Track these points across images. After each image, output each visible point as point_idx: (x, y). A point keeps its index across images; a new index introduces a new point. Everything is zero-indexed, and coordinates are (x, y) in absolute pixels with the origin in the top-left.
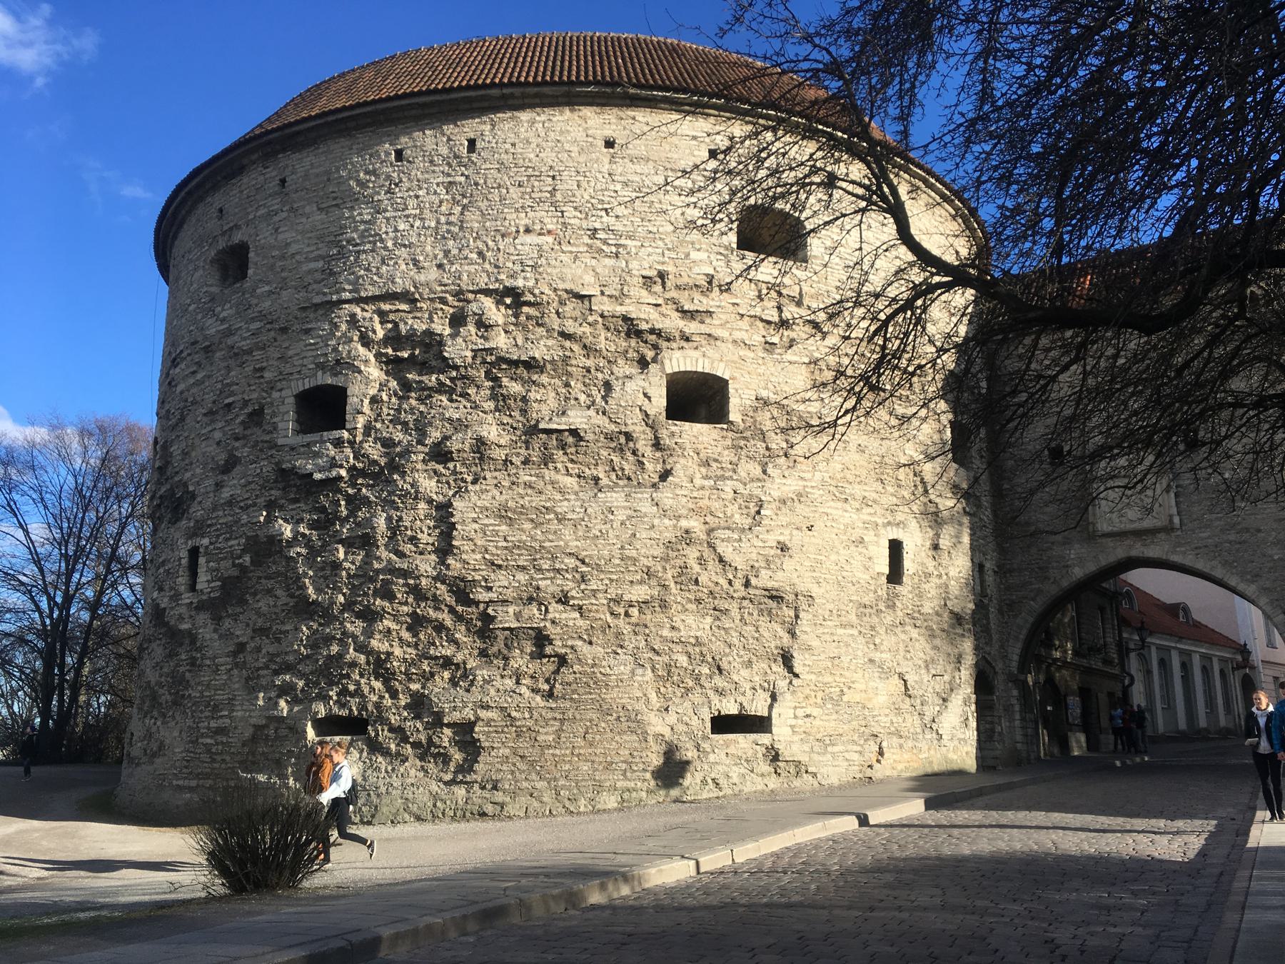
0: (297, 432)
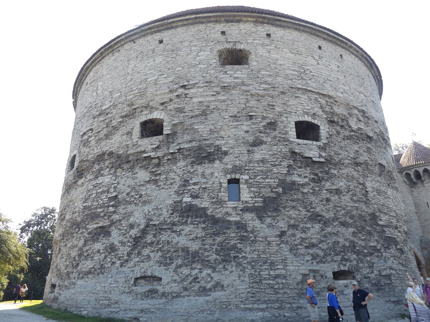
0: (298, 137)
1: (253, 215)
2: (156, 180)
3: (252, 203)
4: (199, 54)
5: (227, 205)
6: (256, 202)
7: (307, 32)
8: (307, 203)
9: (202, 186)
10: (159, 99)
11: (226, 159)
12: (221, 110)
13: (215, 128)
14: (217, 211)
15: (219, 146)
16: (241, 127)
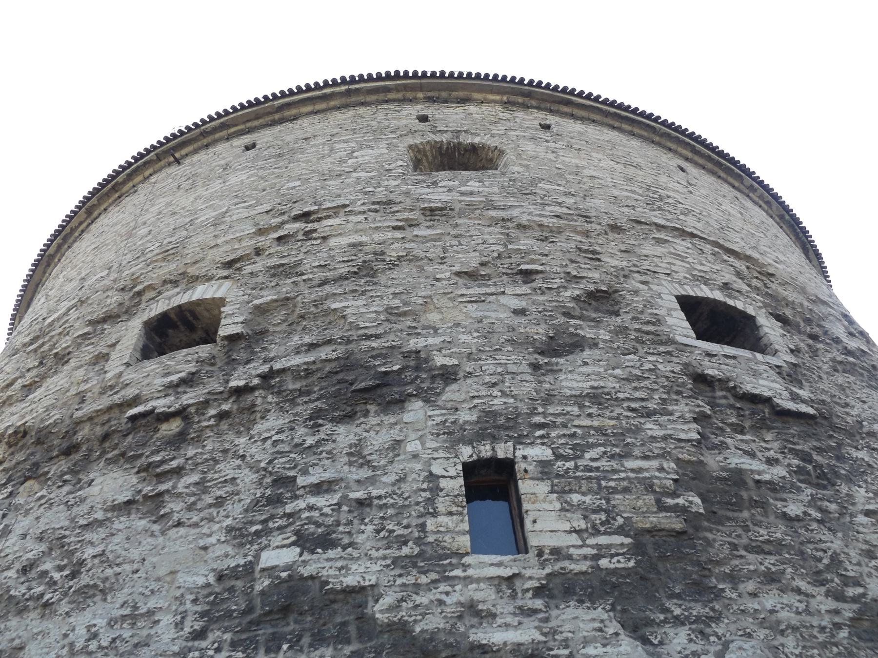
1: (599, 613)
2: (160, 494)
3: (585, 557)
4: (355, 154)
5: (470, 572)
6: (602, 552)
7: (640, 137)
8: (820, 560)
9: (353, 495)
10: (221, 255)
11: (452, 393)
12: (426, 261)
13: (406, 304)
14: (423, 599)
15: (423, 354)
16: (498, 301)
